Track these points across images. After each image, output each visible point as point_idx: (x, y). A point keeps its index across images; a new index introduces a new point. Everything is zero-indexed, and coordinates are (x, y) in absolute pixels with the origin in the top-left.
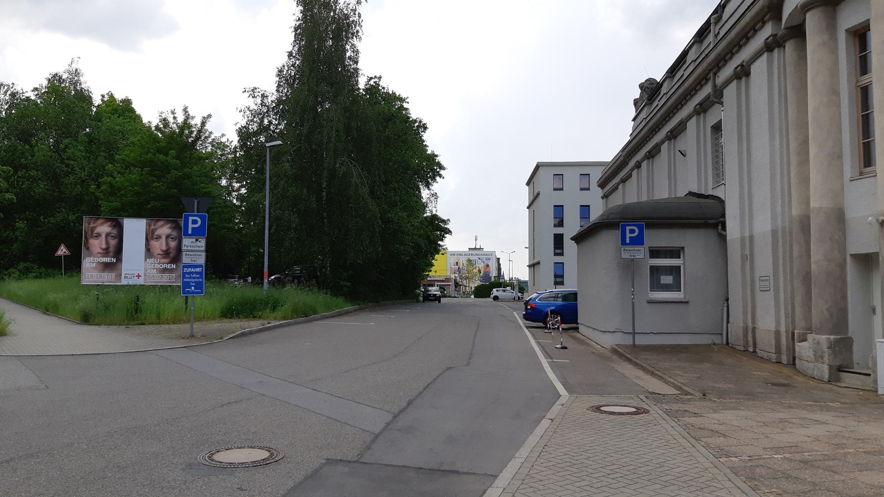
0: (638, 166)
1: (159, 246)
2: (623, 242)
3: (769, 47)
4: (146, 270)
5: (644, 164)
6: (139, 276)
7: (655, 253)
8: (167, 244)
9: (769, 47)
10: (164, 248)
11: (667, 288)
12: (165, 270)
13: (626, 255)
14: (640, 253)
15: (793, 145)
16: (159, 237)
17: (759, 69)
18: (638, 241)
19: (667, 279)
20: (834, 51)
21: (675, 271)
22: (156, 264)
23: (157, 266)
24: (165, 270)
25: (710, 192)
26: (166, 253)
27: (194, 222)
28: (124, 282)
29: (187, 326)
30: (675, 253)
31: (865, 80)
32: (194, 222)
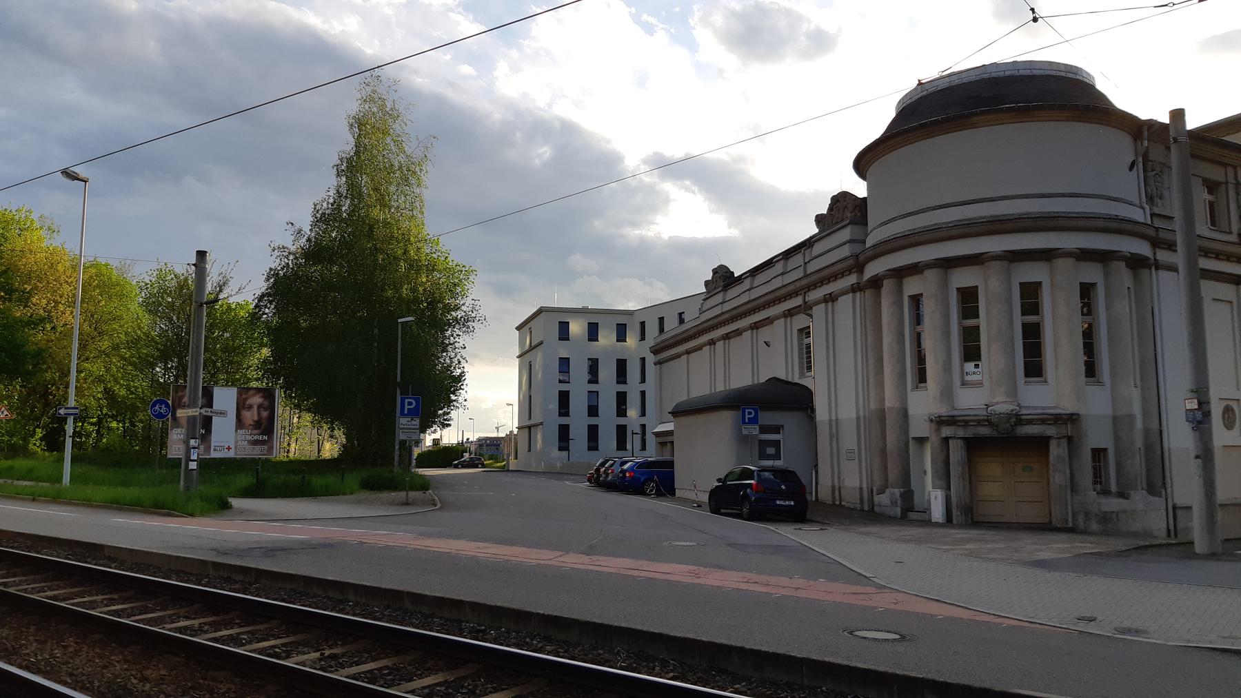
0: (712, 343)
1: (250, 416)
2: (744, 422)
3: (854, 289)
4: (236, 442)
5: (720, 344)
6: (229, 448)
7: (764, 430)
8: (259, 414)
9: (854, 289)
10: (256, 418)
11: (770, 457)
12: (256, 442)
13: (745, 432)
14: (755, 430)
15: (871, 362)
16: (250, 407)
17: (845, 302)
18: (754, 421)
19: (771, 451)
20: (901, 308)
21: (776, 444)
22: (246, 435)
23: (249, 438)
24: (256, 442)
25: (796, 380)
26: (257, 425)
27: (410, 404)
28: (214, 455)
29: (403, 494)
30: (776, 429)
31: (919, 329)
32: (410, 404)
